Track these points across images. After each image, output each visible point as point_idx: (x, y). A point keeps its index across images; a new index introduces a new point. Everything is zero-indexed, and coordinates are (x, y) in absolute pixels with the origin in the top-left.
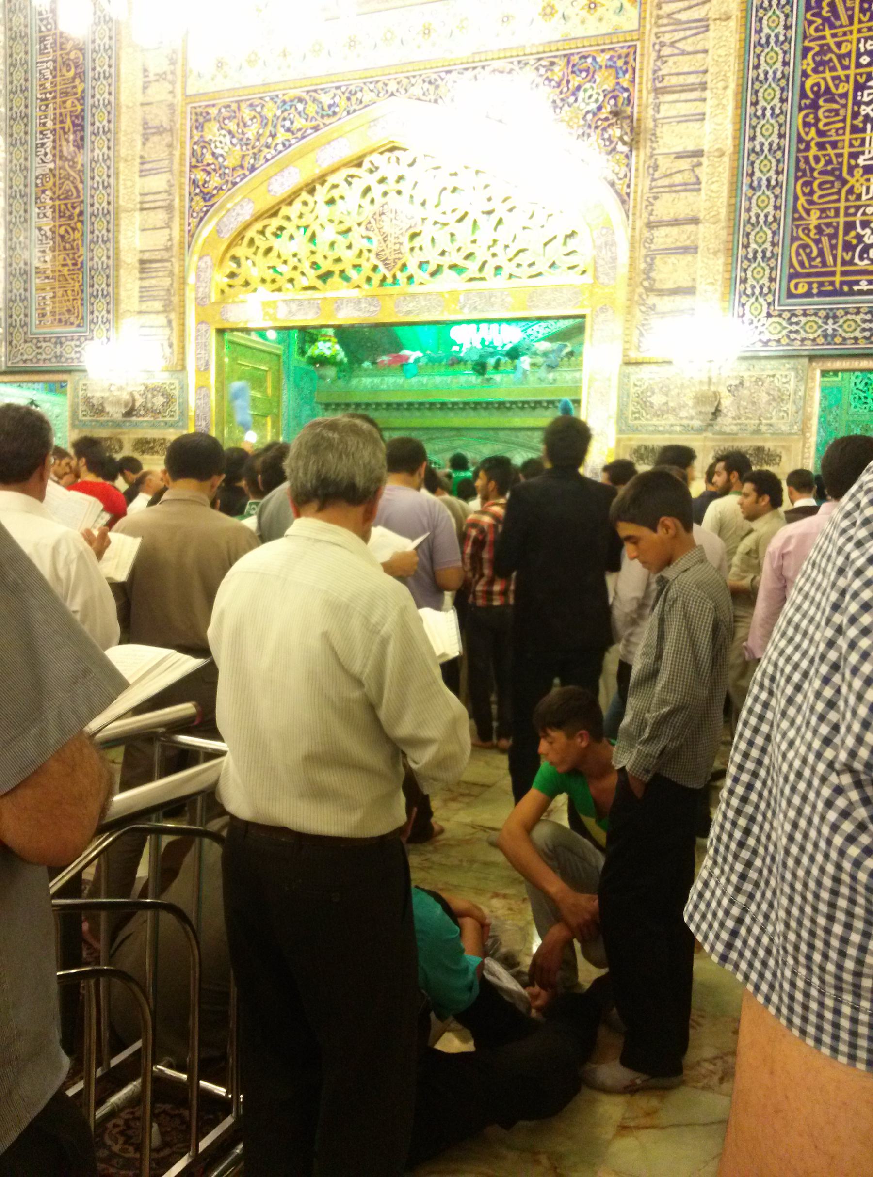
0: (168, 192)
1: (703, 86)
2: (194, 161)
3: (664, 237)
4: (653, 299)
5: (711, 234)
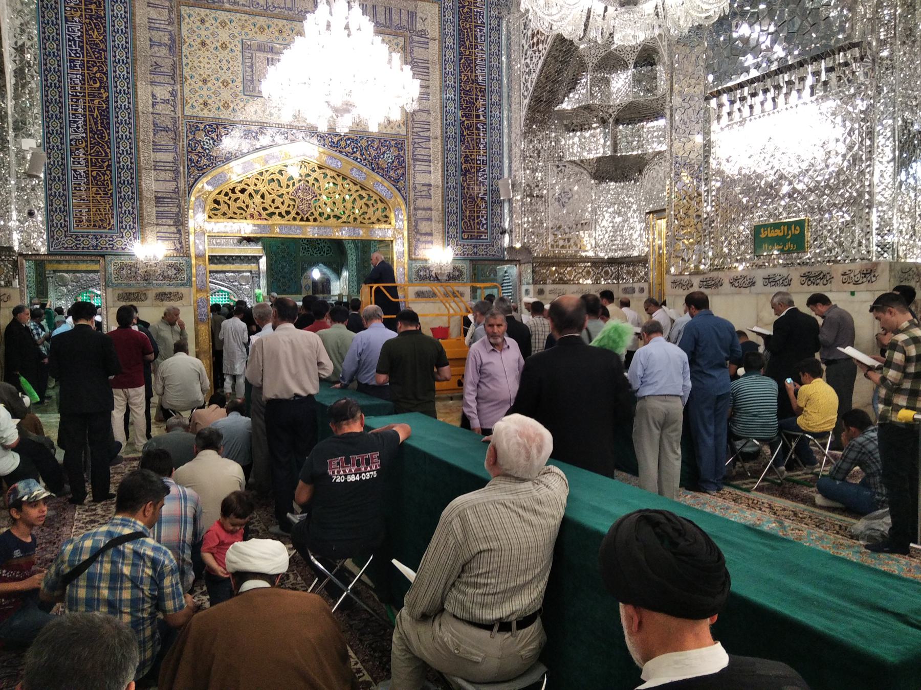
0: (175, 163)
1: (430, 161)
2: (190, 149)
3: (420, 214)
4: (418, 237)
5: (436, 214)
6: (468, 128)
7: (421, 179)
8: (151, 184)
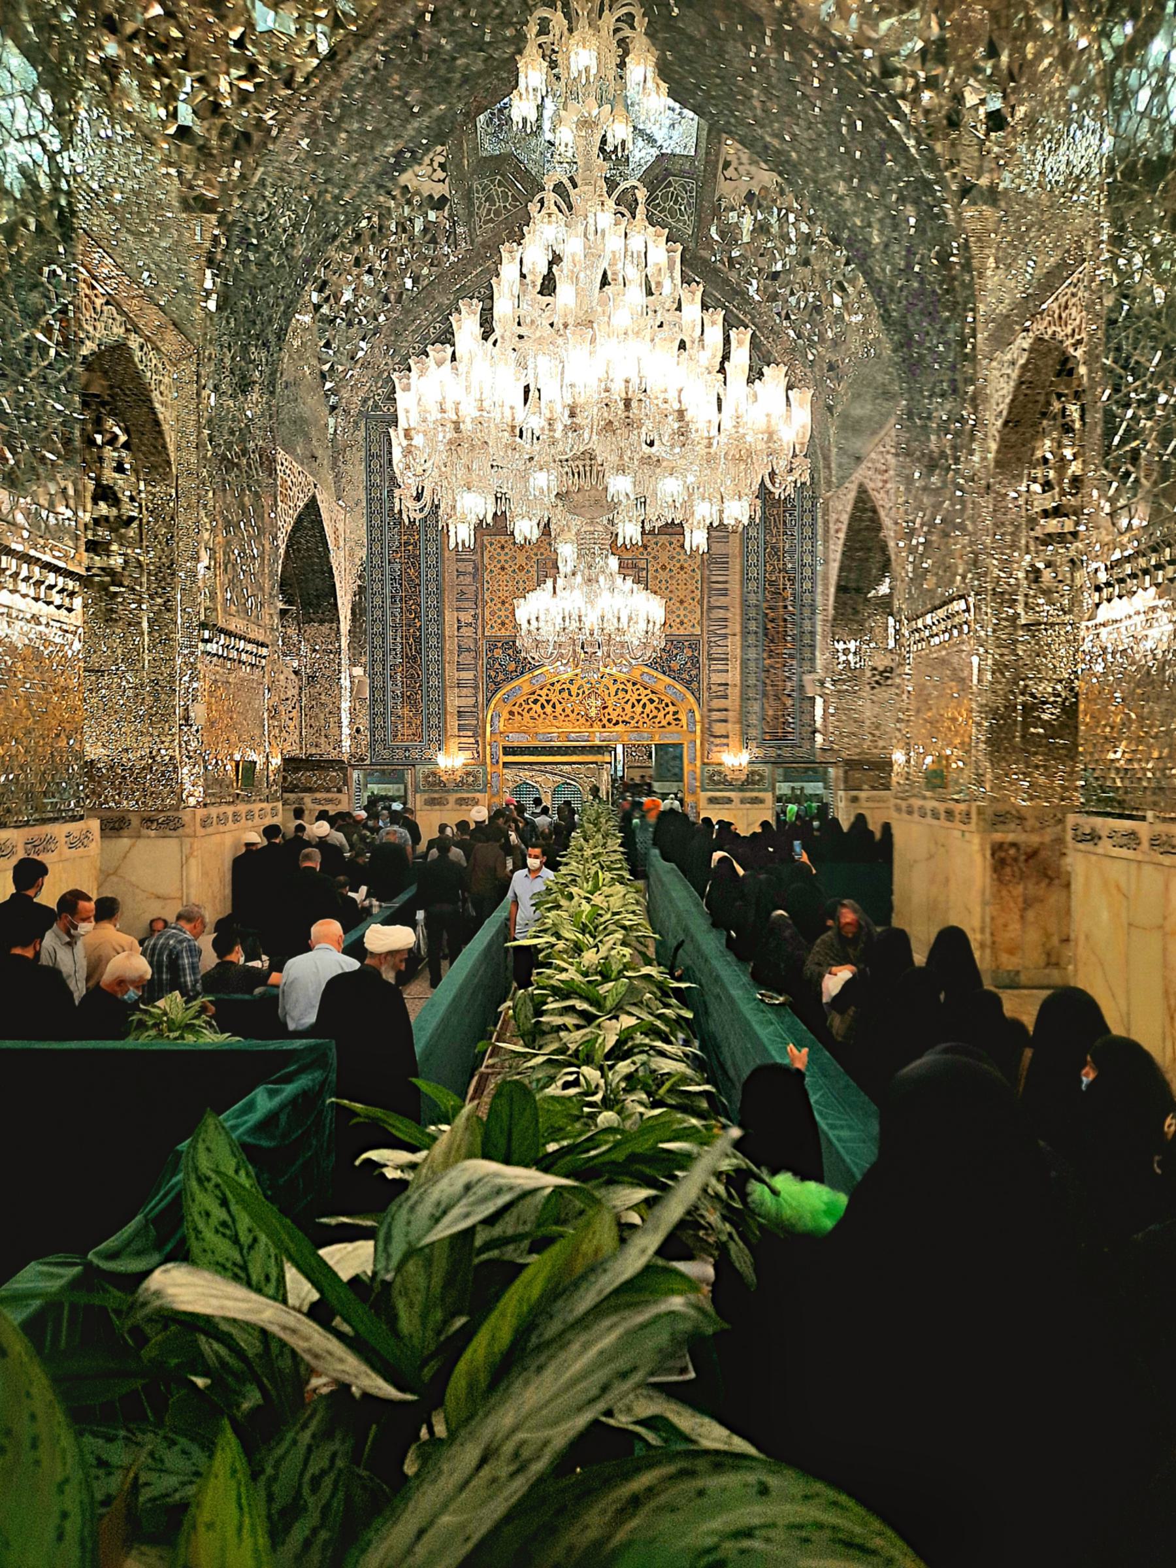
3: (716, 715)
6: (772, 621)
7: (716, 678)
8: (453, 701)
